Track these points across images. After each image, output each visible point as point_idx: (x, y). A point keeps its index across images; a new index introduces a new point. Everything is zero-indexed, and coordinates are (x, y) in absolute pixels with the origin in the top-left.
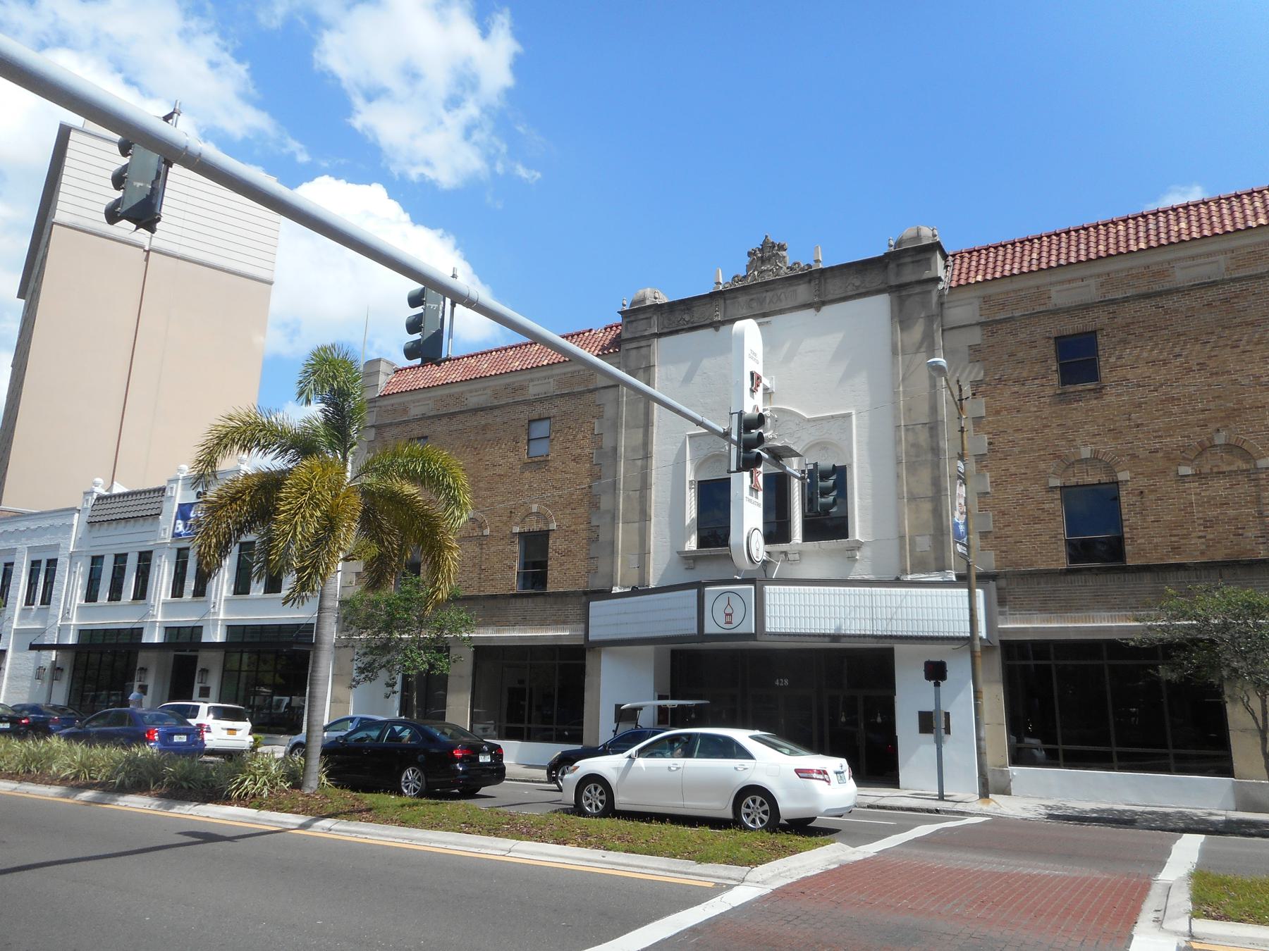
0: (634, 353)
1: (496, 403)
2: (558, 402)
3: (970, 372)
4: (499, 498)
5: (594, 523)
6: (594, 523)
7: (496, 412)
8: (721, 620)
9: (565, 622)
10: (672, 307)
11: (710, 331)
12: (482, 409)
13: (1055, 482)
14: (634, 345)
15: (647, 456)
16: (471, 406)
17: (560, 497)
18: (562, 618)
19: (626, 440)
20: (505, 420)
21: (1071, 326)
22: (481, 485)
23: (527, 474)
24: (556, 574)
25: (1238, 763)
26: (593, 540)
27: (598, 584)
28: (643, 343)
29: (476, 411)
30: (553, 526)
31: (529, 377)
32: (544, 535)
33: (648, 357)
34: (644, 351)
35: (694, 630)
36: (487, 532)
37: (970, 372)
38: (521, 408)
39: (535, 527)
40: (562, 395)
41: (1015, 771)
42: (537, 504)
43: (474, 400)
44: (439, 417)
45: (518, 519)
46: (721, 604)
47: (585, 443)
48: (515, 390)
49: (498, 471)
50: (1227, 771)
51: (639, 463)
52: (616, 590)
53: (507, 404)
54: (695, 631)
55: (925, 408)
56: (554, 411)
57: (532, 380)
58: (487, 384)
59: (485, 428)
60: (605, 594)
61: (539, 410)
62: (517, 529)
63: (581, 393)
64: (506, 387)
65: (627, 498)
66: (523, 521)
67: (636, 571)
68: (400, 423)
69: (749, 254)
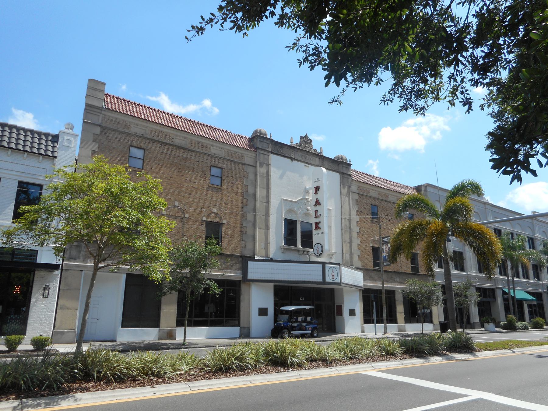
0: (262, 155)
1: (192, 148)
2: (226, 162)
3: (94, 146)
4: (195, 200)
5: (244, 225)
6: (244, 225)
7: (192, 154)
8: (331, 277)
9: (231, 269)
10: (277, 143)
11: (289, 160)
12: (183, 148)
13: (371, 245)
14: (262, 152)
15: (268, 202)
16: (176, 144)
17: (228, 208)
18: (230, 267)
19: (260, 193)
20: (198, 159)
21: (374, 203)
22: (183, 189)
23: (210, 192)
24: (226, 245)
25: (398, 320)
26: (244, 233)
27: (247, 253)
28: (266, 153)
29: (180, 148)
30: (224, 222)
31: (211, 143)
32: (220, 225)
33: (268, 160)
34: (266, 156)
35: (320, 279)
36: (187, 216)
37: (94, 146)
38: (207, 157)
39: (215, 220)
40: (229, 160)
41: (408, 325)
42: (217, 209)
43: (177, 141)
44: (155, 141)
45: (205, 214)
46: (331, 271)
47: (240, 187)
48: (203, 147)
49: (194, 185)
50: (396, 323)
51: (265, 204)
52: (256, 257)
53: (199, 152)
54: (321, 280)
55: (348, 214)
56: (224, 166)
57: (212, 146)
58: (187, 136)
59: (185, 159)
60: (253, 259)
61: (216, 162)
62: (204, 219)
63: (238, 163)
64: (199, 143)
65: (260, 218)
66: (208, 215)
67: (264, 251)
68: (122, 133)
69: (301, 138)
